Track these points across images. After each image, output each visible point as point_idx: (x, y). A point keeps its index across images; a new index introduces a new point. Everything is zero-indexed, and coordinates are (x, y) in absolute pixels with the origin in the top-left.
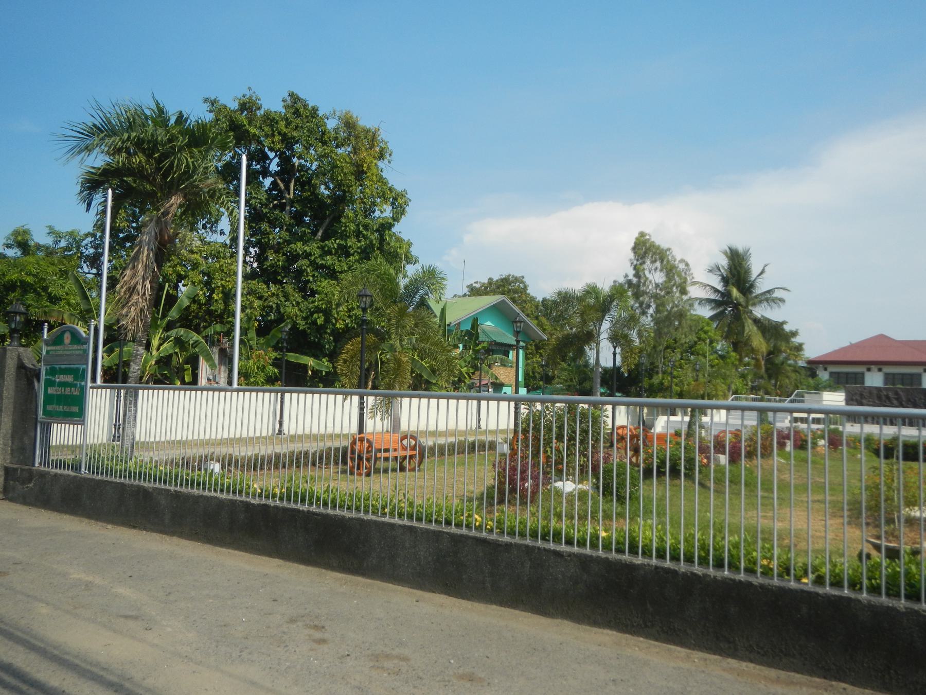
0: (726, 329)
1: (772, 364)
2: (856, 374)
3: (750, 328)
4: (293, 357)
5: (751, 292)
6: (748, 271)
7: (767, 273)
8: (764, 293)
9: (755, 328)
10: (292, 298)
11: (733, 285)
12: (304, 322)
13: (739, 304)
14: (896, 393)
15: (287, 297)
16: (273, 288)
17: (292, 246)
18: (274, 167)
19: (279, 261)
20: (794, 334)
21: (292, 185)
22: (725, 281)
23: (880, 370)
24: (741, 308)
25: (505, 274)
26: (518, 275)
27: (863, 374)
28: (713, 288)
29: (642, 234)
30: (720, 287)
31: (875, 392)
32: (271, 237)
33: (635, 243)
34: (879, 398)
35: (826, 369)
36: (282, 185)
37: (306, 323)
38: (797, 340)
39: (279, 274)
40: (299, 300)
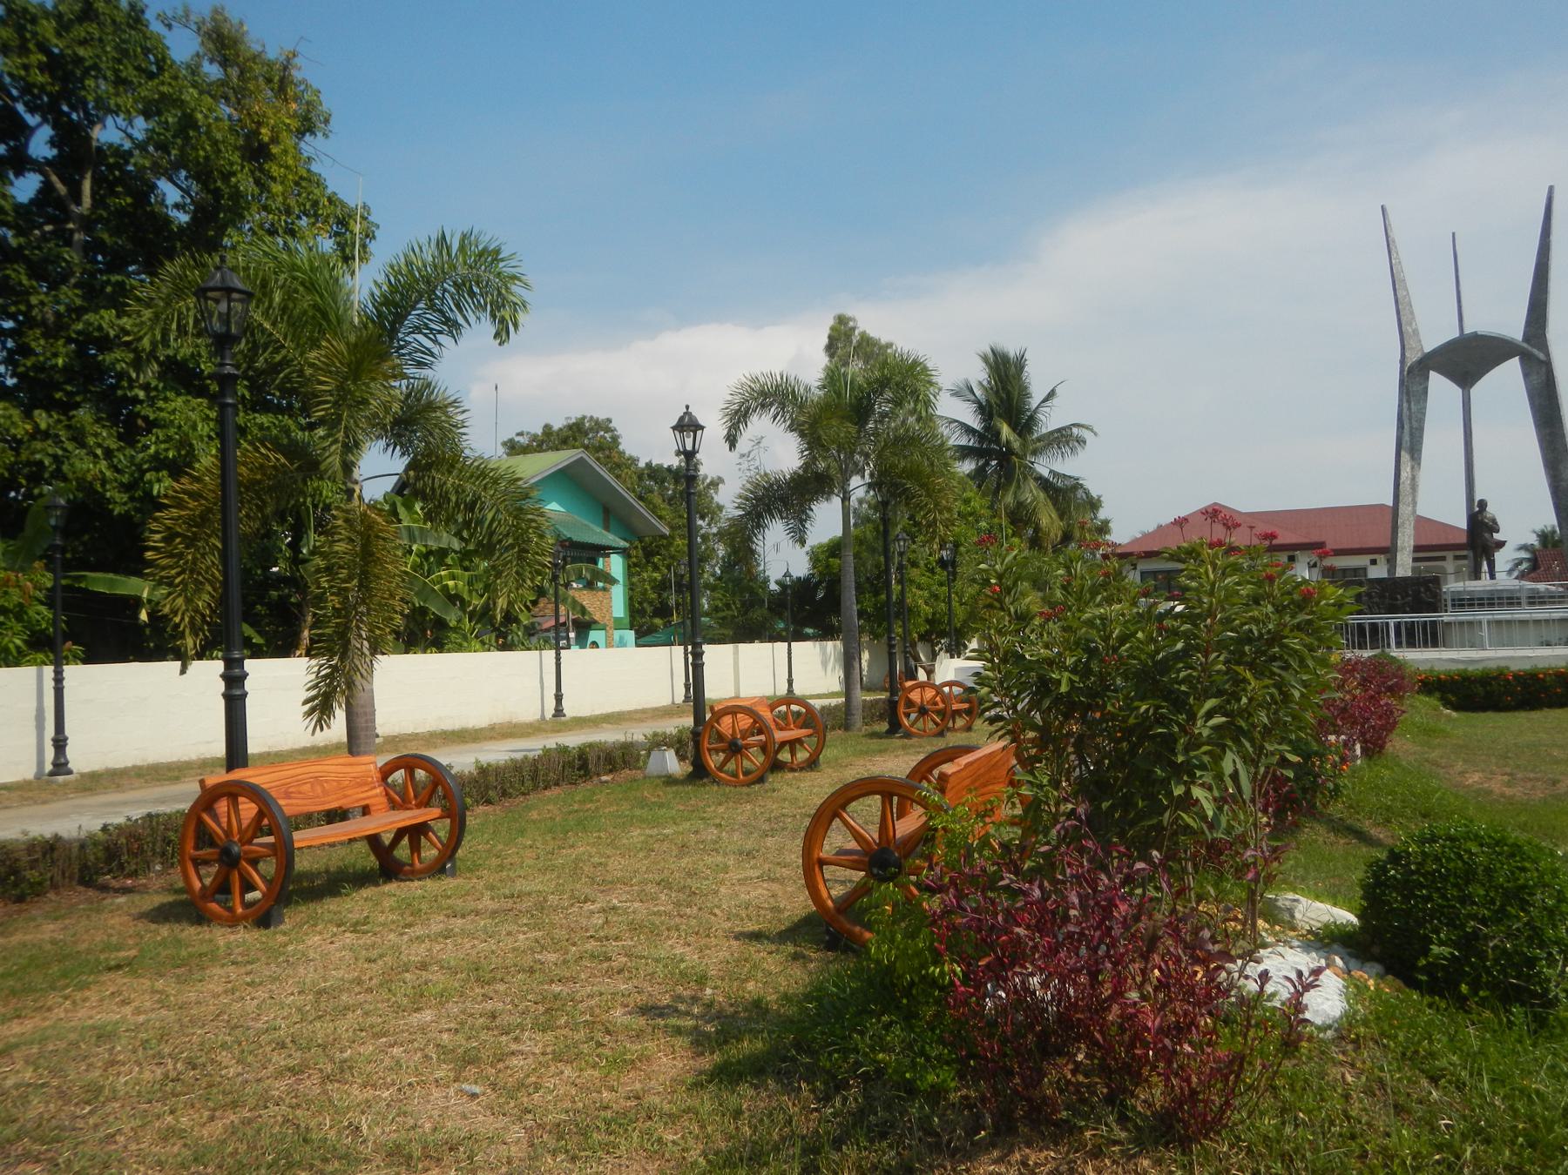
4: (101, 582)
5: (1030, 431)
6: (1024, 393)
8: (1052, 433)
10: (91, 441)
11: (1000, 416)
12: (125, 497)
13: (1011, 452)
15: (79, 438)
16: (42, 419)
17: (90, 317)
18: (40, 145)
19: (55, 355)
21: (87, 186)
22: (984, 410)
25: (574, 415)
26: (602, 416)
29: (841, 320)
32: (34, 300)
33: (830, 337)
36: (61, 189)
37: (132, 499)
39: (58, 387)
40: (113, 444)
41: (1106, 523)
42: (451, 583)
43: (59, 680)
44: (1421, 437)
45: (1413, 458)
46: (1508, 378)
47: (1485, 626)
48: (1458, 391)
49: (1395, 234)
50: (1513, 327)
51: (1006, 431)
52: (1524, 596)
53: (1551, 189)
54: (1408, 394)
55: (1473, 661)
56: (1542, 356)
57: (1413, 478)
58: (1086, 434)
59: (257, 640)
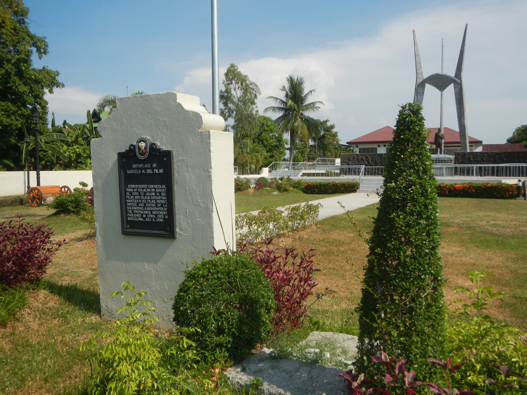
1: (324, 144)
2: (372, 149)
5: (302, 103)
6: (301, 91)
8: (310, 104)
13: (294, 110)
14: (367, 157)
20: (332, 127)
22: (287, 96)
23: (385, 146)
27: (376, 148)
28: (281, 100)
30: (284, 100)
31: (356, 157)
34: (358, 160)
35: (357, 147)
38: (334, 130)
41: (336, 133)
42: (77, 150)
43: (28, 174)
46: (451, 89)
47: (444, 169)
48: (440, 92)
49: (417, 39)
50: (451, 72)
53: (467, 25)
54: (417, 93)
55: (327, 180)
56: (459, 81)
59: (12, 165)
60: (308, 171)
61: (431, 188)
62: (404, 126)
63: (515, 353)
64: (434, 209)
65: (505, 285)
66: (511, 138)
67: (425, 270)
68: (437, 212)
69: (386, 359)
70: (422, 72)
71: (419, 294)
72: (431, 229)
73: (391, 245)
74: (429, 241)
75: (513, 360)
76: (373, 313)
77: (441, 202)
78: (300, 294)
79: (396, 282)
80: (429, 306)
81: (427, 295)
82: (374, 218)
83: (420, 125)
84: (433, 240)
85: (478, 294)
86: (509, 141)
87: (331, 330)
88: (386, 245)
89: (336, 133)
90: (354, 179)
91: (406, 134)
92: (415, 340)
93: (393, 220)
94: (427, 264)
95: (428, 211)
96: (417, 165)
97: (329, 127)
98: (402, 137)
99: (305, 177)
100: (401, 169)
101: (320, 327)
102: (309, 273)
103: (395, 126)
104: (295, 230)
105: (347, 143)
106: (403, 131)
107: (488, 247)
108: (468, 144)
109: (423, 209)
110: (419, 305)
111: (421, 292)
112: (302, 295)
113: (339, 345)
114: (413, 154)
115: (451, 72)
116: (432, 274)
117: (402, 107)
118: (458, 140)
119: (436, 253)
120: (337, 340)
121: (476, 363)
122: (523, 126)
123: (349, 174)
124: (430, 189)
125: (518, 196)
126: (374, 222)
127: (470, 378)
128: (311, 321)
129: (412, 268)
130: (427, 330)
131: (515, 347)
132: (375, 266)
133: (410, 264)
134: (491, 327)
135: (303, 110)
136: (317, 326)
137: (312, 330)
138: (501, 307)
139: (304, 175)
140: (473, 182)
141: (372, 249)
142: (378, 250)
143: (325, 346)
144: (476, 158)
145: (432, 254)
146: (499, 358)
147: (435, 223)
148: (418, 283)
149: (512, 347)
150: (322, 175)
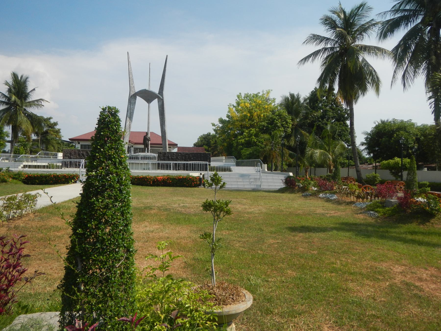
0: (8, 118)
1: (47, 139)
3: (22, 118)
5: (25, 99)
7: (38, 90)
9: (25, 119)
14: (87, 153)
20: (56, 124)
22: (10, 91)
24: (18, 107)
30: (7, 94)
31: (77, 152)
34: (79, 155)
35: (79, 143)
38: (57, 127)
41: (59, 130)
44: (133, 114)
45: (130, 119)
46: (155, 102)
50: (156, 90)
51: (14, 98)
52: (140, 157)
54: (130, 103)
56: (162, 98)
57: (130, 125)
58: (43, 103)
60: (30, 164)
61: (125, 176)
62: (104, 125)
63: (188, 300)
64: (128, 193)
65: (188, 251)
66: (197, 143)
67: (119, 244)
68: (130, 196)
69: (80, 327)
70: (134, 87)
71: (114, 265)
72: (125, 210)
73: (91, 225)
74: (123, 220)
75: (187, 306)
76: (73, 287)
77: (133, 189)
78: (8, 281)
79: (95, 257)
80: (122, 273)
81: (121, 265)
82: (77, 203)
83: (117, 125)
84: (126, 219)
85: (163, 258)
86: (195, 145)
87: (40, 310)
88: (87, 225)
89: (59, 130)
90: (74, 171)
91: (105, 131)
92: (110, 304)
93: (93, 203)
94: (121, 239)
95: (122, 195)
96: (114, 157)
97: (52, 124)
98: (102, 133)
99: (27, 169)
100: (100, 160)
101: (29, 310)
102: (18, 259)
103: (97, 124)
104: (11, 219)
105: (70, 139)
106: (103, 128)
107: (178, 223)
108: (167, 146)
109: (118, 194)
110: (114, 274)
111: (116, 263)
112: (10, 281)
113: (45, 323)
114: (111, 148)
115: (156, 90)
116: (125, 247)
117: (102, 109)
118: (161, 143)
119: (128, 229)
120: (44, 318)
121: (162, 314)
122: (204, 135)
123: (70, 167)
124: (124, 177)
125: (199, 185)
126: (77, 206)
127: (156, 327)
128: (20, 306)
129: (109, 243)
130: (120, 294)
131: (188, 296)
132: (76, 245)
133: (106, 240)
134: (172, 283)
135: (26, 106)
136: (26, 310)
137: (19, 314)
138: (185, 268)
139: (25, 166)
140: (170, 175)
141: (74, 230)
142: (80, 231)
143: (31, 327)
144: (173, 156)
145: (125, 230)
146: (177, 307)
147: (128, 205)
148: (113, 256)
149: (186, 296)
150: (44, 167)
